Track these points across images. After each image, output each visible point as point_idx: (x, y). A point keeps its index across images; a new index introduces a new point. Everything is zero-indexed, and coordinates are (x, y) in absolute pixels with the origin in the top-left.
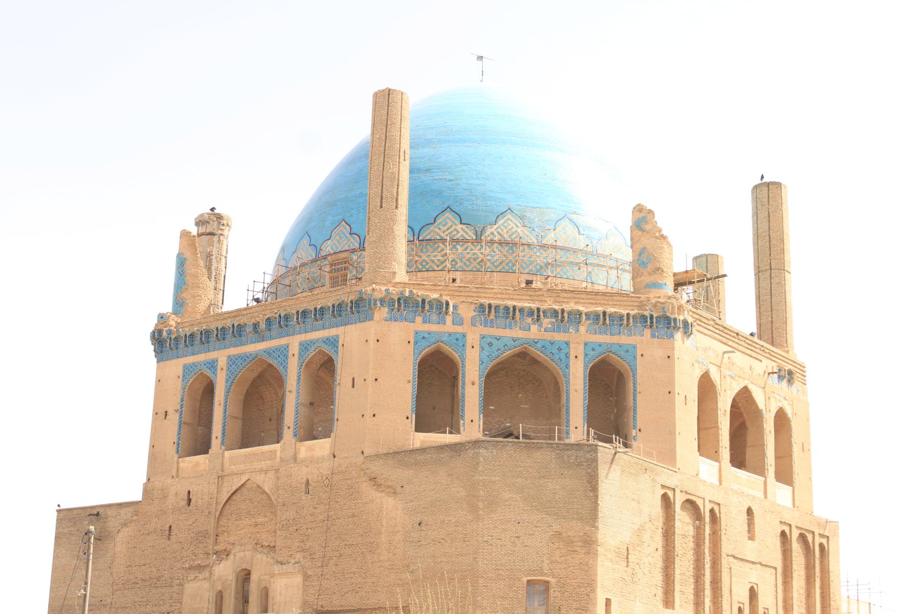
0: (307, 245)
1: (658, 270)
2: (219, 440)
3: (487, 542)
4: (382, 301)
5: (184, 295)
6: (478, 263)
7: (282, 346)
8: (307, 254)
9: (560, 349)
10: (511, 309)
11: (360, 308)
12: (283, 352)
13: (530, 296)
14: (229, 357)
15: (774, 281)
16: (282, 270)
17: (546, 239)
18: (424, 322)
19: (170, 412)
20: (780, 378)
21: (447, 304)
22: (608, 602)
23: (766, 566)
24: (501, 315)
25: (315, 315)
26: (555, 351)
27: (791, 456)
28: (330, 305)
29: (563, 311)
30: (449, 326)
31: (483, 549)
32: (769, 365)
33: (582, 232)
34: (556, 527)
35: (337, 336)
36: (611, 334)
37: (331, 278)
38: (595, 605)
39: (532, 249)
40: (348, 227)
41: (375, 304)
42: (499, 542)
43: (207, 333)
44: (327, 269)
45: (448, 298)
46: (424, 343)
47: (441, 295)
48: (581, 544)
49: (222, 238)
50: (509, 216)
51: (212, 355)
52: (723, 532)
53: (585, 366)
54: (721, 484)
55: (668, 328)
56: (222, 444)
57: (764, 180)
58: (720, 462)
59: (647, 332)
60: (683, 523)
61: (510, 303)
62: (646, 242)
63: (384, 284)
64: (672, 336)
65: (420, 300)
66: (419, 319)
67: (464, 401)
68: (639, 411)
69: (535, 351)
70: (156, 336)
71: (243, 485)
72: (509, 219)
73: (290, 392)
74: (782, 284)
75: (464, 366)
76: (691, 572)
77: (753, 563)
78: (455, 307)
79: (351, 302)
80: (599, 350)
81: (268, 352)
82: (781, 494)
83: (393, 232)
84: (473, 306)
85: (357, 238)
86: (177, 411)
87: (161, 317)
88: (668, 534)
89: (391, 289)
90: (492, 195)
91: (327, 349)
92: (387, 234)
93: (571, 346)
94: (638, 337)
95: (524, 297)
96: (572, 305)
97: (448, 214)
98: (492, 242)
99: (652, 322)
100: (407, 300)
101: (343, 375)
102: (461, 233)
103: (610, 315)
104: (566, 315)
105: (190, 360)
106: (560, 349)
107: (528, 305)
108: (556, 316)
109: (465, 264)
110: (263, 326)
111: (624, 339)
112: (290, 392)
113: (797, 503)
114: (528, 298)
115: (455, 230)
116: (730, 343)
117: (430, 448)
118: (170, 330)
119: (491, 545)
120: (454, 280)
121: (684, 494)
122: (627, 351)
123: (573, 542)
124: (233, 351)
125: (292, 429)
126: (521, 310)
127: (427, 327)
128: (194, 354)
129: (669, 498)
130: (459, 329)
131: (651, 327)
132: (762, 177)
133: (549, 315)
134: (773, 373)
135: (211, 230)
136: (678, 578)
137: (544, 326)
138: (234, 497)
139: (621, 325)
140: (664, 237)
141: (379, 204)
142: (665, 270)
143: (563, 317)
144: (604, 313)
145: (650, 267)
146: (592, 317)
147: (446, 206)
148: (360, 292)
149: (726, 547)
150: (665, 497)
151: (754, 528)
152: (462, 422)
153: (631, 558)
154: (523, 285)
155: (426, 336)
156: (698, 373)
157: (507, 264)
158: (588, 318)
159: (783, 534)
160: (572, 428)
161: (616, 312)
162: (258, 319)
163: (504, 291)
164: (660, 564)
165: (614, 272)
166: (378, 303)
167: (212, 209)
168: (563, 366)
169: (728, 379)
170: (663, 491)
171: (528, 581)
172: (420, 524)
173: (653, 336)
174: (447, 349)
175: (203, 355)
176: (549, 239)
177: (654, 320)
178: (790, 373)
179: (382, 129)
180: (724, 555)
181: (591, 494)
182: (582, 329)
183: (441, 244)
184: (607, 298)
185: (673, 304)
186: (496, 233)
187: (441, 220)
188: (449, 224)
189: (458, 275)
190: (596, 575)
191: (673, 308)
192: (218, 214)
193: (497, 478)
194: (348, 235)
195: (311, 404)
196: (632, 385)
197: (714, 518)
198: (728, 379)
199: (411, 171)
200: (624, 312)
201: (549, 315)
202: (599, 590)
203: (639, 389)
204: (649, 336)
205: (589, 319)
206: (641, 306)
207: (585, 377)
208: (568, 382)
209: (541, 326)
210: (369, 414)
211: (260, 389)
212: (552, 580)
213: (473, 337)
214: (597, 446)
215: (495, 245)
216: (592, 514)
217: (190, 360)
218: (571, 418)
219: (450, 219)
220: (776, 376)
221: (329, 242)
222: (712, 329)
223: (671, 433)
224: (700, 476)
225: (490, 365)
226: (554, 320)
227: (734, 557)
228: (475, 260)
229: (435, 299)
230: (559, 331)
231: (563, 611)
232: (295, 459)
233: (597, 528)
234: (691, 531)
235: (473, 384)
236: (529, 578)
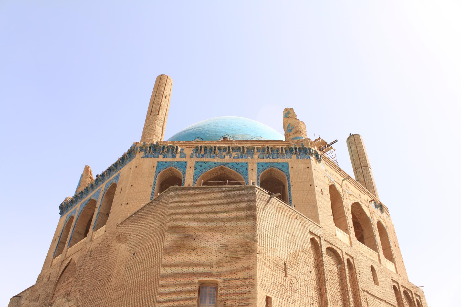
3: (169, 253)
4: (141, 149)
15: (364, 171)
21: (177, 148)
22: (268, 300)
23: (389, 303)
26: (239, 167)
27: (390, 247)
29: (243, 147)
31: (165, 258)
34: (224, 241)
38: (255, 299)
42: (178, 253)
46: (162, 167)
48: (243, 252)
52: (358, 275)
53: (258, 174)
54: (351, 245)
55: (306, 154)
58: (349, 234)
59: (294, 157)
60: (329, 263)
62: (290, 121)
65: (162, 146)
66: (161, 156)
71: (69, 263)
74: (368, 172)
76: (339, 296)
77: (381, 300)
80: (265, 166)
82: (389, 265)
83: (155, 123)
84: (192, 149)
88: (319, 266)
103: (271, 148)
104: (245, 150)
106: (242, 166)
111: (280, 160)
113: (398, 272)
119: (172, 255)
121: (327, 243)
122: (283, 166)
123: (236, 251)
126: (219, 148)
127: (165, 160)
129: (317, 242)
130: (183, 160)
133: (236, 150)
136: (329, 296)
137: (233, 156)
138: (65, 271)
139: (278, 154)
143: (243, 150)
146: (261, 151)
149: (362, 285)
150: (312, 240)
151: (377, 279)
153: (289, 272)
154: (222, 139)
155: (164, 163)
159: (394, 287)
164: (314, 283)
166: (139, 149)
168: (245, 174)
170: (312, 236)
171: (199, 281)
172: (134, 254)
173: (298, 158)
180: (361, 289)
181: (251, 218)
182: (256, 156)
185: (307, 141)
190: (256, 275)
191: (307, 143)
193: (181, 210)
196: (287, 182)
197: (351, 267)
201: (236, 150)
202: (259, 288)
203: (291, 184)
204: (295, 158)
205: (259, 152)
209: (231, 156)
212: (220, 281)
213: (191, 163)
216: (252, 231)
223: (315, 206)
224: (337, 236)
226: (239, 153)
227: (368, 293)
229: (170, 146)
231: (228, 305)
233: (256, 241)
234: (336, 270)
236: (200, 279)
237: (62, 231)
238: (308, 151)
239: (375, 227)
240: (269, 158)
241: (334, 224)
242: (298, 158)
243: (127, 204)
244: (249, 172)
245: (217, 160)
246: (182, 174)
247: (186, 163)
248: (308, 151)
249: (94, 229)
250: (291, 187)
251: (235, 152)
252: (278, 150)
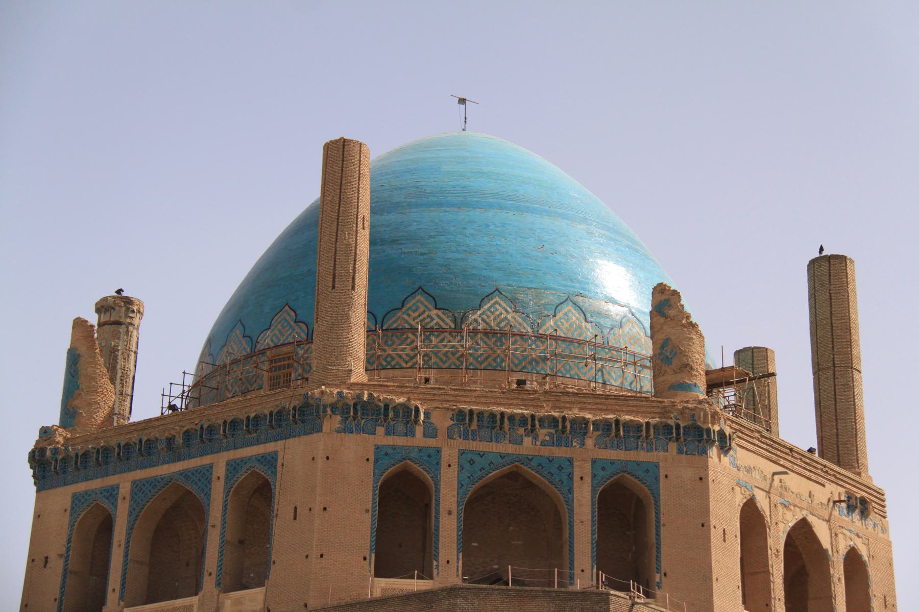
0: (240, 337)
1: (687, 368)
4: (333, 407)
5: (76, 402)
6: (458, 359)
7: (204, 466)
8: (240, 348)
9: (560, 468)
10: (499, 417)
11: (306, 417)
12: (205, 474)
13: (522, 400)
14: (134, 482)
16: (208, 369)
17: (544, 328)
18: (388, 433)
19: (53, 556)
20: (851, 508)
21: (417, 410)
24: (486, 424)
25: (247, 426)
26: (554, 470)
28: (267, 412)
29: (564, 418)
30: (419, 439)
32: (837, 491)
33: (590, 319)
35: (276, 453)
36: (626, 449)
37: (270, 379)
39: (526, 341)
40: (292, 314)
41: (325, 411)
43: (106, 451)
44: (266, 366)
45: (418, 403)
47: (409, 399)
49: (131, 328)
50: (497, 299)
51: (111, 480)
53: (594, 490)
55: (699, 441)
57: (824, 253)
59: (673, 447)
61: (496, 409)
63: (337, 386)
64: (704, 452)
65: (382, 405)
66: (381, 430)
67: (437, 536)
68: (664, 549)
69: (530, 472)
70: (37, 457)
72: (496, 303)
73: (214, 526)
75: (438, 491)
78: (427, 414)
79: (294, 408)
81: (185, 474)
83: (348, 318)
84: (450, 414)
85: (304, 327)
86: (61, 556)
87: (46, 433)
89: (345, 391)
90: (475, 272)
91: (261, 469)
92: (342, 320)
93: (576, 464)
94: (661, 453)
95: (515, 402)
96: (576, 411)
97: (419, 297)
98: (475, 332)
99: (678, 434)
100: (365, 405)
101: (282, 505)
102: (437, 320)
104: (568, 424)
105: (82, 487)
106: (560, 468)
107: (520, 411)
108: (556, 426)
109: (441, 359)
110: (179, 440)
111: (642, 456)
112: (214, 526)
114: (520, 402)
115: (429, 316)
116: (782, 462)
117: (392, 598)
118: (56, 449)
120: (427, 380)
122: (647, 471)
124: (140, 474)
125: (214, 576)
126: (512, 418)
127: (391, 440)
128: (87, 480)
130: (432, 442)
131: (677, 440)
132: (821, 249)
133: (546, 424)
134: (840, 501)
135: (117, 319)
137: (541, 438)
139: (639, 437)
140: (693, 326)
141: (331, 284)
142: (695, 366)
143: (564, 427)
144: (617, 422)
145: (675, 363)
147: (416, 287)
148: (306, 396)
152: (435, 563)
154: (514, 386)
155: (390, 451)
156: (739, 500)
157: (494, 360)
158: (596, 428)
160: (577, 571)
161: (631, 421)
162: (173, 432)
163: (490, 394)
165: (630, 370)
166: (329, 409)
167: (119, 291)
169: (780, 508)
173: (680, 452)
174: (417, 468)
175: (99, 480)
176: (549, 326)
177: (682, 431)
178: (863, 501)
179: (334, 190)
182: (589, 442)
183: (410, 335)
184: (620, 403)
185: (705, 411)
186: (480, 320)
187: (411, 304)
188: (422, 308)
189: (432, 374)
191: (706, 415)
192: (127, 298)
194: (292, 323)
195: (241, 542)
196: (654, 515)
198: (780, 508)
199: (373, 242)
200: (642, 420)
201: (546, 424)
203: (663, 520)
204: (675, 451)
206: (664, 412)
207: (593, 505)
208: (571, 511)
209: (536, 438)
210: (315, 553)
211: (174, 523)
213: (450, 453)
214: (609, 594)
215: (479, 335)
217: (82, 487)
218: (576, 557)
219: (422, 303)
220: (844, 505)
221: (268, 332)
222: (757, 442)
225: (472, 489)
226: (553, 431)
228: (453, 354)
229: (401, 405)
230: (559, 445)
235: (450, 513)
237: (69, 541)
238: (705, 437)
239: (838, 571)
240: (619, 447)
241: (741, 607)
243: (322, 556)
244: (575, 485)
245: (506, 447)
246: (433, 485)
247: (438, 451)
248: (705, 437)
249: (218, 584)
250: (662, 528)
251: (545, 428)
252: (639, 426)
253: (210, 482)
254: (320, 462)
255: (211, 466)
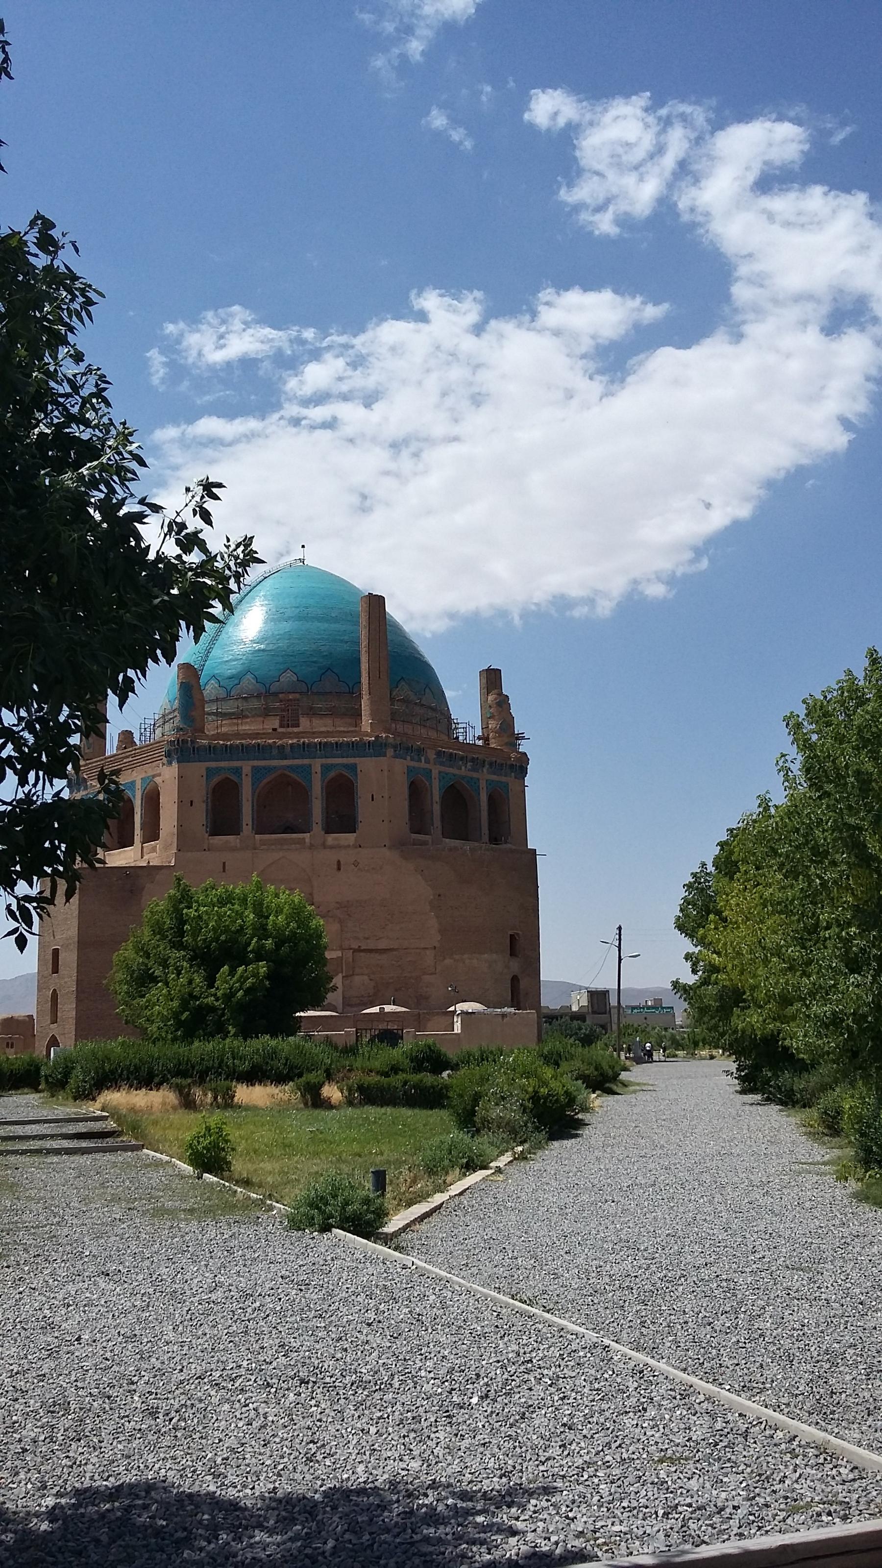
2: (250, 827)
14: (253, 767)
35: (356, 764)
56: (253, 828)
84: (434, 752)
105: (213, 764)
111: (503, 779)
124: (256, 763)
127: (413, 764)
130: (427, 766)
173: (516, 778)
213: (435, 773)
217: (213, 764)
232: (324, 846)
242: (516, 778)
253: (310, 774)
254: (386, 773)
255: (310, 765)
